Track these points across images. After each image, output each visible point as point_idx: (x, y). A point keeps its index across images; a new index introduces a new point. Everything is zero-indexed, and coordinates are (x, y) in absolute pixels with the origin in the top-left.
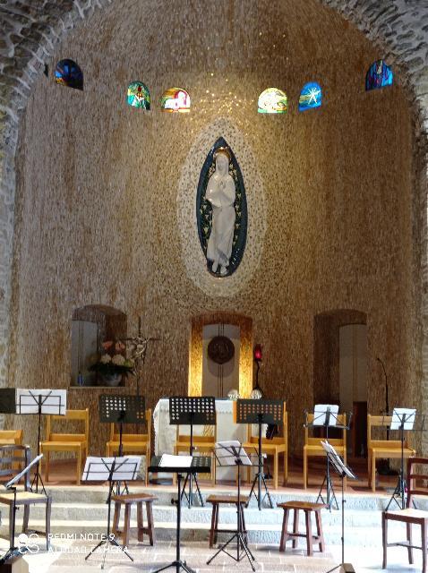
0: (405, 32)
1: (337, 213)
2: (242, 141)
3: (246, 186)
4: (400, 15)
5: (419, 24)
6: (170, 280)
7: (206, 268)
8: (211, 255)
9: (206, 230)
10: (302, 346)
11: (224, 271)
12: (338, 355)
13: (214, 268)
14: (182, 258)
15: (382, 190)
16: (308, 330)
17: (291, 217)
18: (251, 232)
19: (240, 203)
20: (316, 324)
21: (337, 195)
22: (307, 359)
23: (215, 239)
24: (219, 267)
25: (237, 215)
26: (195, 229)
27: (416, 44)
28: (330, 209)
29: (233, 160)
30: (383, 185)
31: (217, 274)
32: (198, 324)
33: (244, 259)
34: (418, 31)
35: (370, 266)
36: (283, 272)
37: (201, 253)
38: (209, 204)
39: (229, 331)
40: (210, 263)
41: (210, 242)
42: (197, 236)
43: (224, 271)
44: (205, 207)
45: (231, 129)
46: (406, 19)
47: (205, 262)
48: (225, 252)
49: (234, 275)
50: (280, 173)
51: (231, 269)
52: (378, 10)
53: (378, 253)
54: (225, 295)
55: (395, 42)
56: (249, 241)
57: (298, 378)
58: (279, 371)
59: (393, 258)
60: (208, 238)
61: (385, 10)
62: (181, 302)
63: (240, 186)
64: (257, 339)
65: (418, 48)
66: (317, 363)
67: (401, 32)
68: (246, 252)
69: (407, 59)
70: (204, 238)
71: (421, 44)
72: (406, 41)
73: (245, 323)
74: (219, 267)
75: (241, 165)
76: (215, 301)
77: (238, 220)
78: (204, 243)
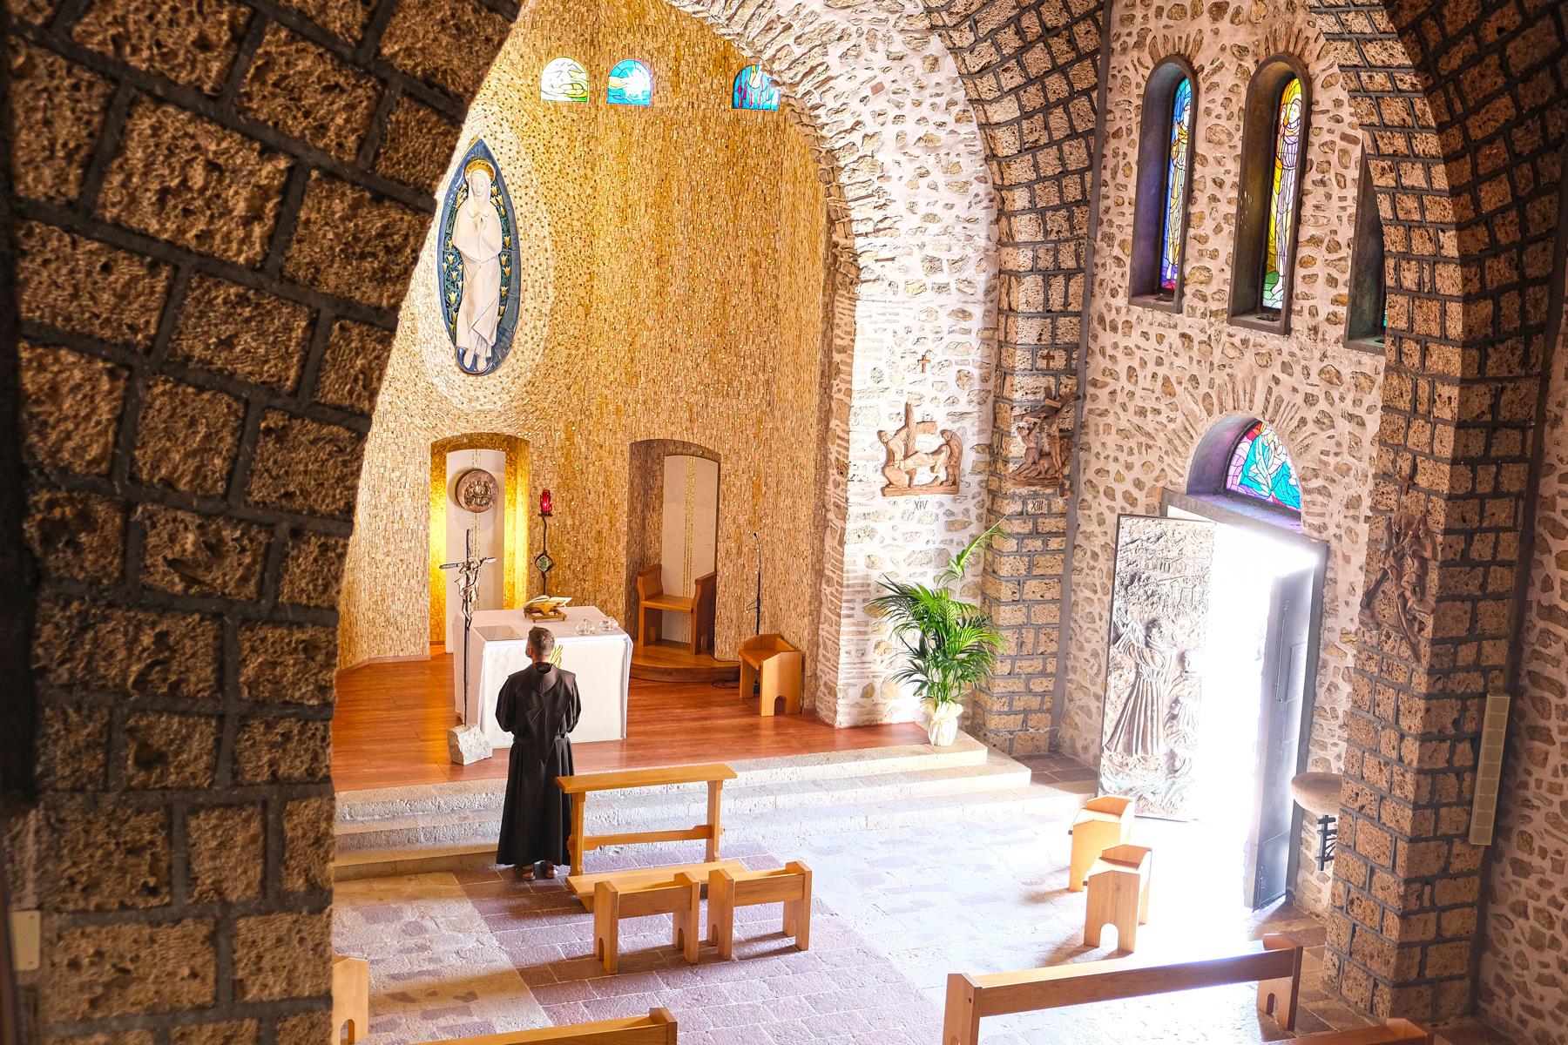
0: (837, 105)
1: (676, 289)
2: (515, 148)
3: (520, 223)
4: (830, 78)
5: (855, 92)
6: (398, 385)
7: (453, 362)
8: (463, 341)
9: (453, 297)
10: (607, 485)
11: (482, 365)
12: (660, 497)
13: (468, 362)
14: (417, 349)
15: (755, 273)
16: (619, 463)
17: (591, 279)
18: (528, 303)
19: (510, 256)
20: (632, 453)
21: (676, 261)
22: (616, 507)
23: (469, 315)
24: (476, 357)
25: (503, 272)
26: (437, 299)
27: (848, 126)
28: (663, 282)
29: (497, 179)
30: (755, 267)
31: (472, 371)
32: (440, 450)
33: (515, 345)
34: (855, 104)
35: (730, 384)
36: (578, 367)
37: (446, 336)
38: (459, 254)
39: (488, 460)
40: (460, 356)
41: (461, 317)
42: (439, 309)
43: (482, 365)
44: (451, 258)
45: (496, 127)
46: (840, 85)
47: (453, 351)
48: (486, 335)
49: (498, 372)
50: (575, 208)
51: (495, 361)
52: (803, 69)
53: (744, 367)
54: (487, 407)
55: (823, 119)
56: (525, 317)
57: (599, 532)
58: (569, 522)
59: (767, 381)
60: (457, 310)
61: (813, 69)
62: (417, 421)
63: (508, 225)
64: (536, 475)
65: (853, 129)
66: (632, 510)
67: (831, 104)
68: (519, 335)
69: (837, 146)
70: (450, 311)
71: (858, 123)
72: (838, 117)
73: (510, 445)
74: (476, 357)
75: (511, 188)
76: (471, 417)
77: (506, 281)
78: (451, 321)
